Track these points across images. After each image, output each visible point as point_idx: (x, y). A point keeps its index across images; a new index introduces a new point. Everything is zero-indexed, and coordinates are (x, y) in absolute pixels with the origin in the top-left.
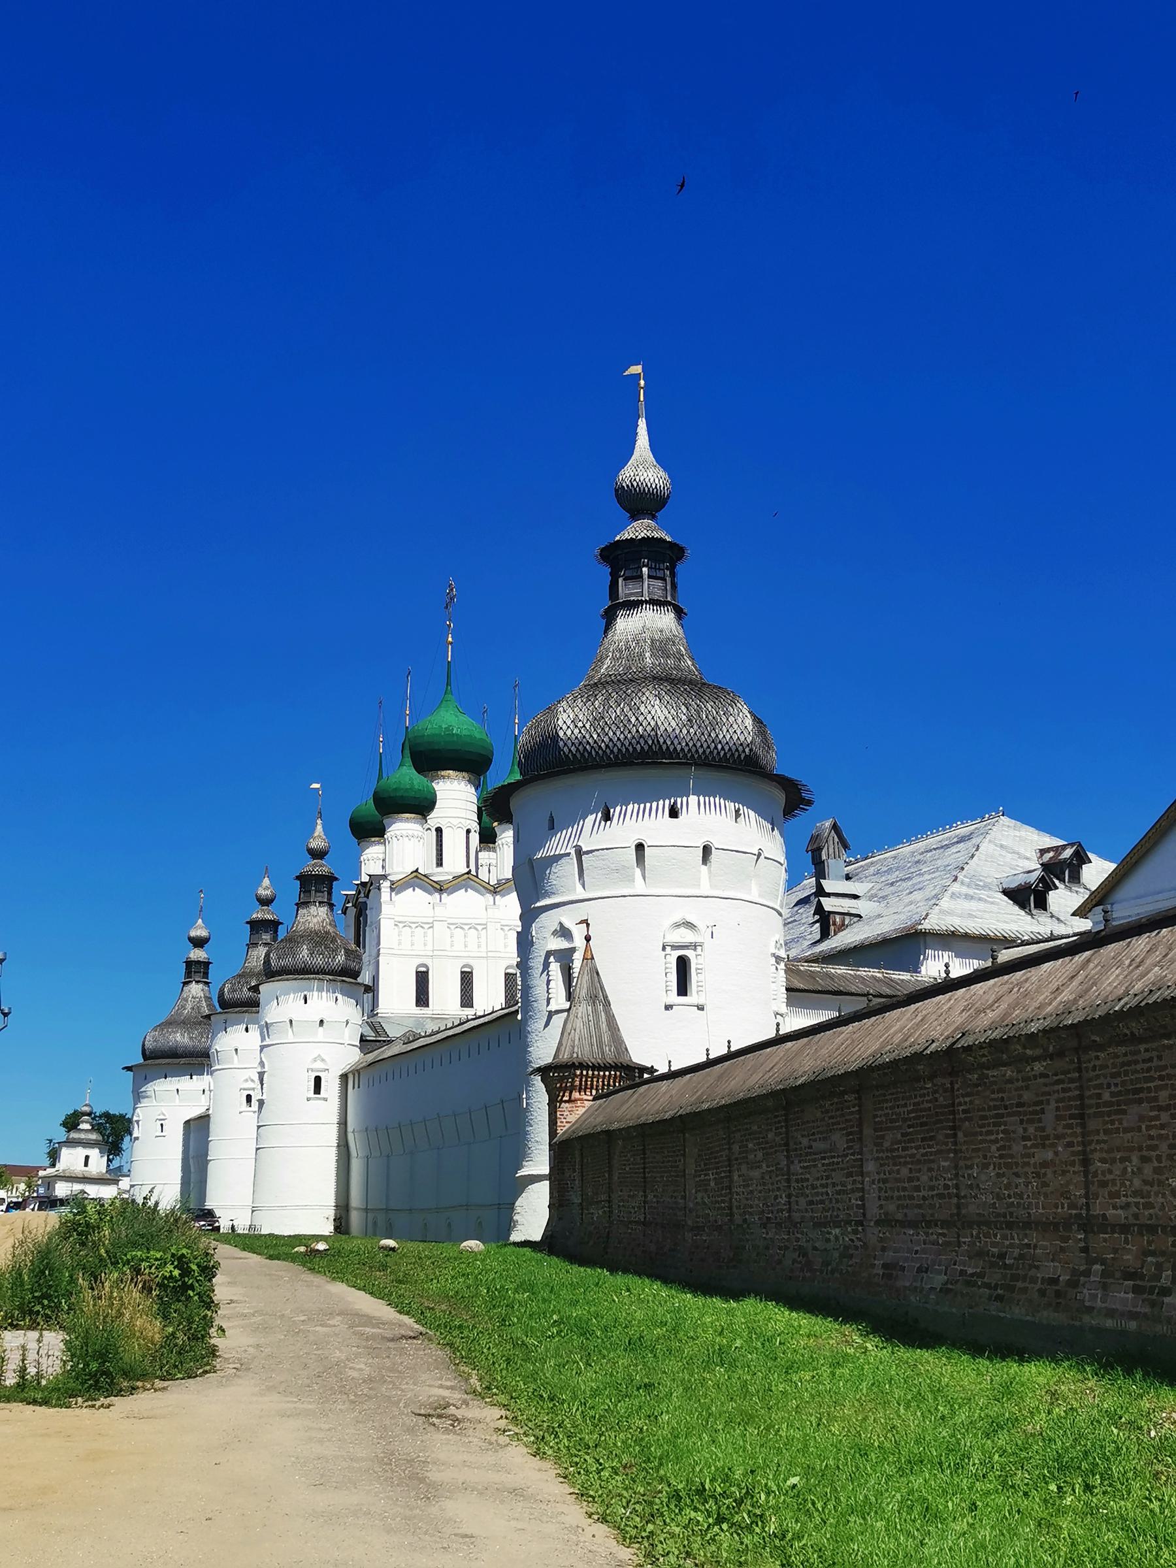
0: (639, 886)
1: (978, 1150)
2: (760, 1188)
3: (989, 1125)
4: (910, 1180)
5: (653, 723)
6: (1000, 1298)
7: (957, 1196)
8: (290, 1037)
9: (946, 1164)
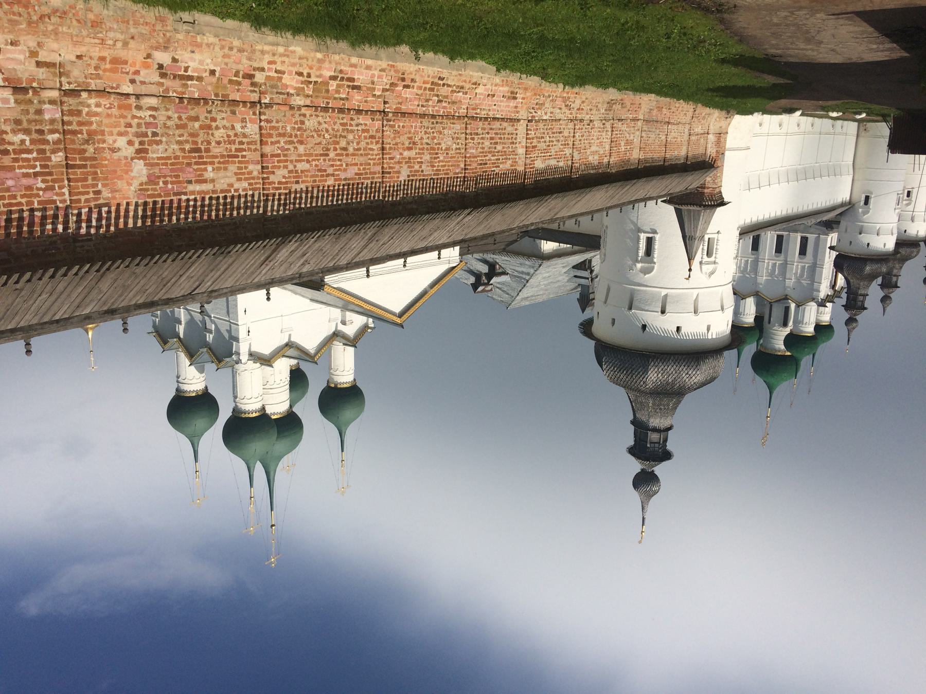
1: (451, 157)
2: (593, 141)
3: (443, 170)
4: (496, 143)
6: (441, 79)
7: (466, 134)
9: (471, 151)
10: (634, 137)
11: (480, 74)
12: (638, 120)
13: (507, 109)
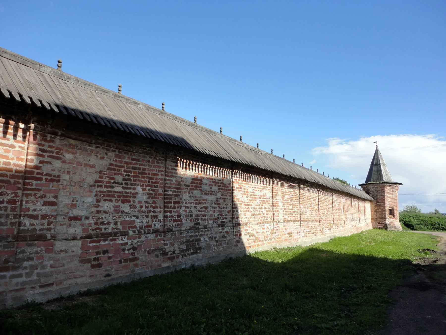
4: (292, 209)
11: (306, 241)
13: (290, 227)
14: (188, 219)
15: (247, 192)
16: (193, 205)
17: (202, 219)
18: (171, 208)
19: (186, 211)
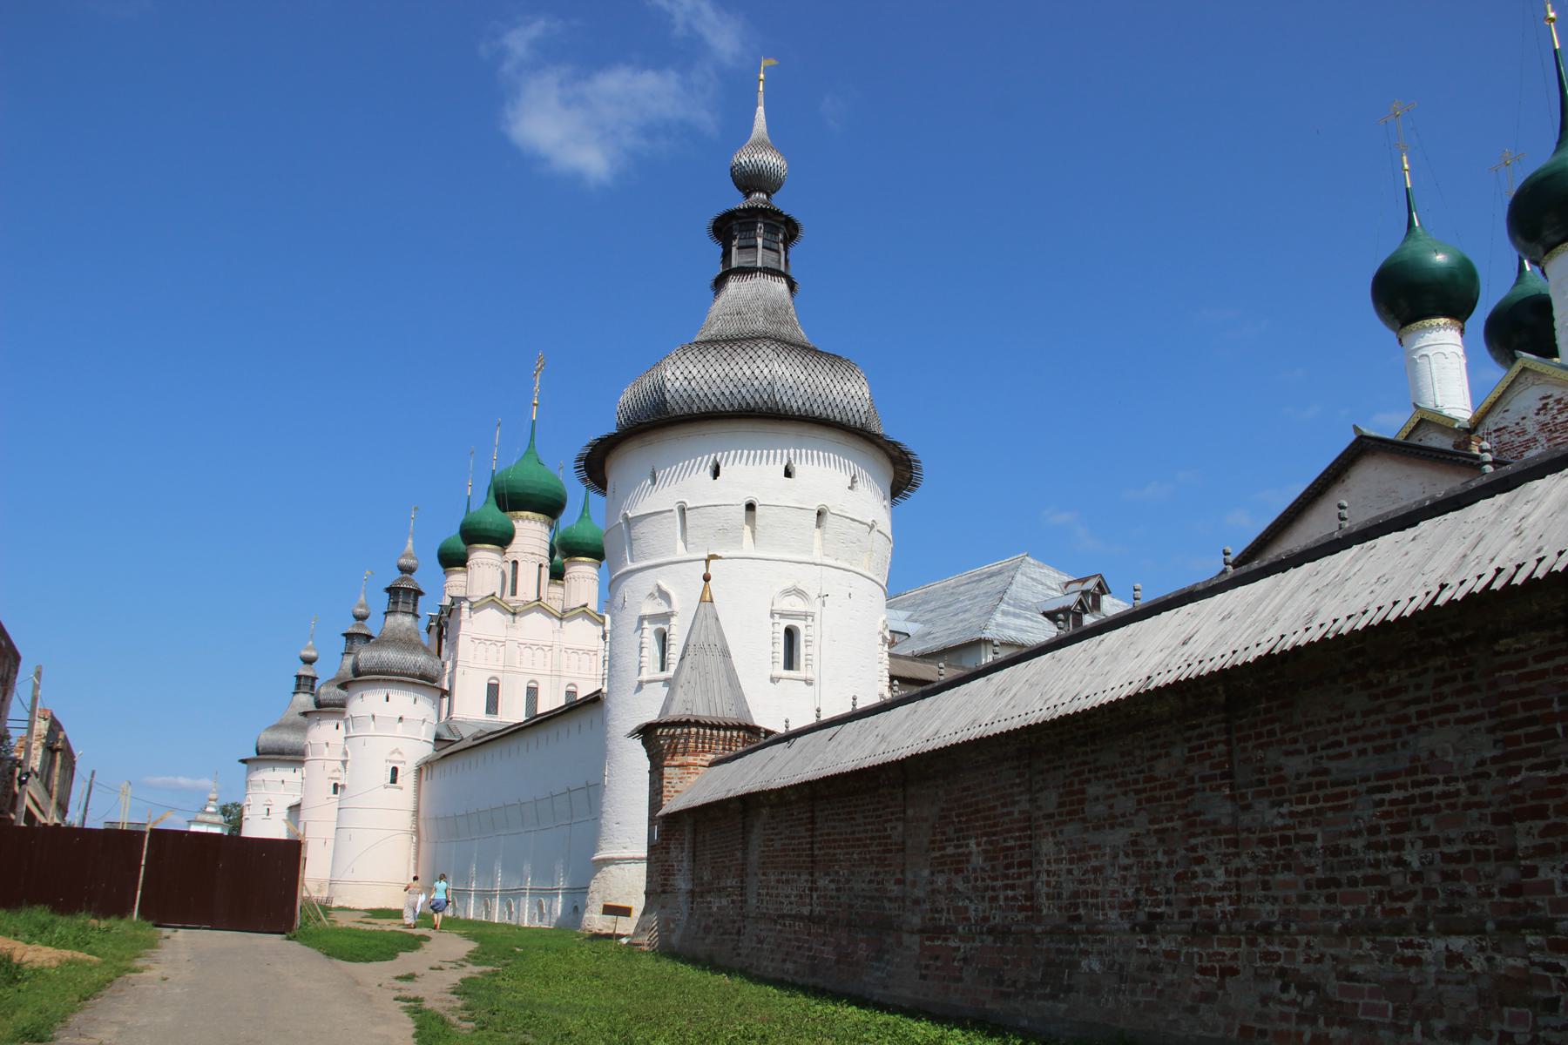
0: (748, 547)
5: (769, 377)
8: (372, 731)
10: (932, 883)
12: (921, 931)
14: (1053, 904)
15: (1282, 779)
16: (1064, 866)
17: (1086, 904)
18: (1014, 879)
19: (1048, 884)
